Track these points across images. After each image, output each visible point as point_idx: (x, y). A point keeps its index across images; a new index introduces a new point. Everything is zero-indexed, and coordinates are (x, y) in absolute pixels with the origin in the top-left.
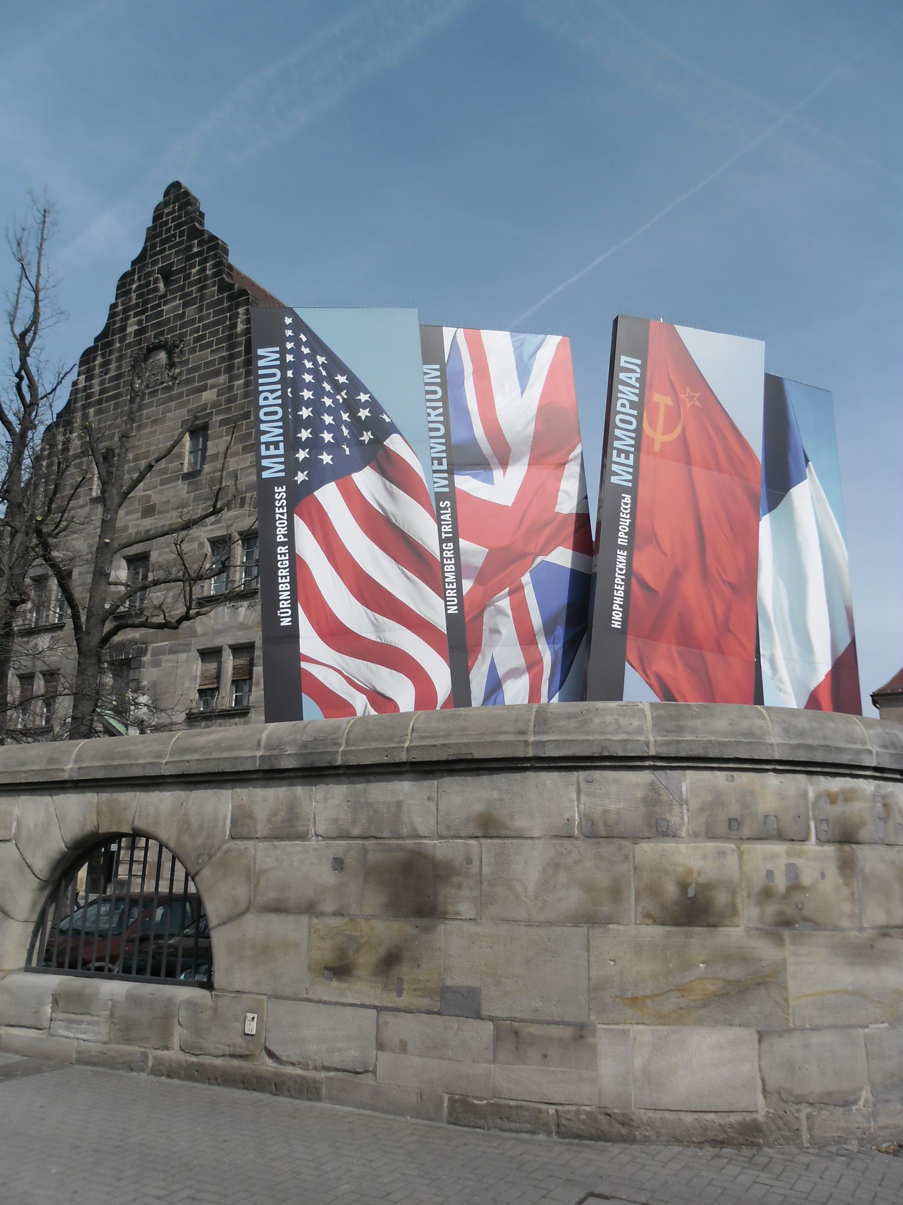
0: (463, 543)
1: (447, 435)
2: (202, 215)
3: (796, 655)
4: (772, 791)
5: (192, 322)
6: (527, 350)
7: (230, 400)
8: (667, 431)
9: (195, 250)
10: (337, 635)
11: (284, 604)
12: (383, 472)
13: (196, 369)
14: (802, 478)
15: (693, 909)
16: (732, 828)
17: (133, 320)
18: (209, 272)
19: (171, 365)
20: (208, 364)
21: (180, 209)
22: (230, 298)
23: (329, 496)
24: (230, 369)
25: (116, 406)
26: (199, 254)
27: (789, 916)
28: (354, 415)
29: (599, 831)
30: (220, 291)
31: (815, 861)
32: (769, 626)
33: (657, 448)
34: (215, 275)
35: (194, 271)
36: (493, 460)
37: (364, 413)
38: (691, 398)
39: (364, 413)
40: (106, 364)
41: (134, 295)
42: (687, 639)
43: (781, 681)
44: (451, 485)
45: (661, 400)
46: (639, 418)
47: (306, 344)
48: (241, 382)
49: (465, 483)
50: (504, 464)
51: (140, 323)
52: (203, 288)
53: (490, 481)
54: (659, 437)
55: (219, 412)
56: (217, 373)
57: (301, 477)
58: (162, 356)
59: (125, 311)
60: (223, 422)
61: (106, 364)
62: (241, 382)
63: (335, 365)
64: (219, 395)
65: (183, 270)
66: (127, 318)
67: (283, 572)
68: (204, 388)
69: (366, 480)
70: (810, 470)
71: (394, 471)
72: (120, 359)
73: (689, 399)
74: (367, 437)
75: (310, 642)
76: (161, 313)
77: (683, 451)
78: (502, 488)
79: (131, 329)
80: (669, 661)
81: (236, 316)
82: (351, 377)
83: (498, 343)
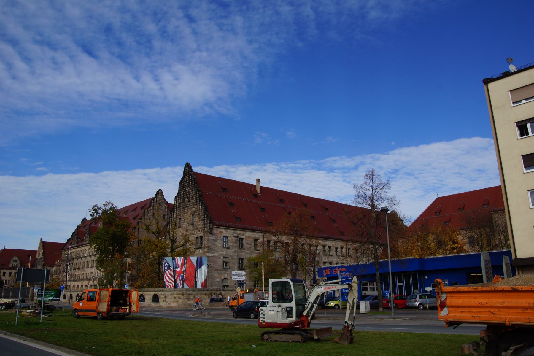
4: (179, 292)
10: (168, 281)
15: (175, 298)
16: (177, 294)
23: (167, 272)
27: (180, 298)
29: (171, 294)
31: (181, 296)
42: (189, 281)
69: (169, 270)
71: (171, 270)
78: (179, 270)
80: (188, 282)
83: (179, 258)
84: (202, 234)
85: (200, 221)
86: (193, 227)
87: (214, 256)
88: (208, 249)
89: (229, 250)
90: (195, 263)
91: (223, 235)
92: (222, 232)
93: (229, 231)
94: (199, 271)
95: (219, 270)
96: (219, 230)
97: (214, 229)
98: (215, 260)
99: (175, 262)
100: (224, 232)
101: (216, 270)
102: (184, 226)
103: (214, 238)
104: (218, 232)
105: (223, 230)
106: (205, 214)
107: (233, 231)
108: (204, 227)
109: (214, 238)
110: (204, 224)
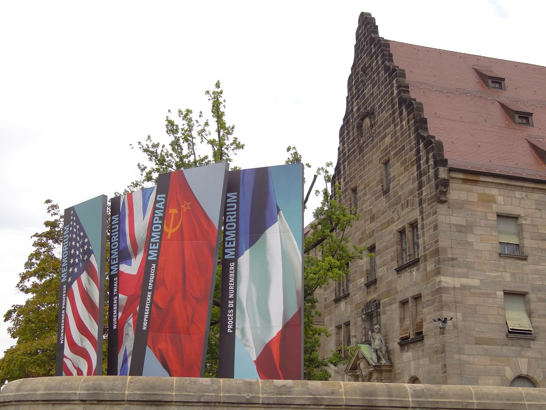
0: (120, 295)
1: (118, 248)
2: (376, 27)
3: (258, 325)
5: (377, 96)
6: (147, 196)
7: (396, 140)
8: (174, 227)
9: (373, 51)
11: (62, 335)
12: (88, 273)
13: (381, 125)
14: (274, 221)
17: (355, 103)
18: (380, 63)
19: (372, 126)
20: (385, 120)
21: (365, 29)
22: (390, 75)
23: (75, 286)
24: (394, 120)
25: (355, 157)
26: (375, 52)
28: (83, 250)
30: (385, 73)
32: (242, 311)
33: (169, 237)
34: (383, 62)
35: (374, 64)
36: (132, 254)
37: (86, 247)
38: (186, 206)
39: (86, 247)
40: (348, 133)
41: (354, 88)
43: (247, 341)
44: (118, 270)
45: (173, 211)
46: (162, 224)
47: (75, 221)
48: (399, 127)
49: (124, 268)
50: (136, 255)
51: (358, 104)
52: (378, 74)
53: (130, 264)
54: (170, 231)
55: (393, 149)
56: (388, 126)
57: (70, 280)
58: (367, 121)
59: (352, 98)
60: (396, 154)
61: (348, 133)
62: (399, 127)
63: (81, 229)
64: (391, 138)
65: (370, 65)
66: (353, 103)
67: (63, 321)
68: (385, 136)
70: (280, 216)
72: (353, 129)
73: (185, 206)
74: (86, 257)
75: (67, 351)
76: (364, 96)
77: (180, 235)
79: (355, 110)
81: (392, 87)
82: (84, 233)
84: (415, 214)
85: (406, 169)
86: (388, 199)
87: (463, 287)
88: (439, 262)
89: (528, 267)
90: (214, 213)
91: (496, 208)
92: (492, 200)
93: (518, 194)
94: (245, 260)
95: (491, 342)
96: (478, 189)
97: (453, 185)
98: (471, 301)
99: (121, 222)
100: (500, 199)
101: (479, 341)
102: (366, 207)
103: (457, 219)
104: (474, 198)
105: (494, 191)
106: (419, 137)
107: (536, 196)
108: (420, 186)
109: (457, 219)
110: (420, 175)
